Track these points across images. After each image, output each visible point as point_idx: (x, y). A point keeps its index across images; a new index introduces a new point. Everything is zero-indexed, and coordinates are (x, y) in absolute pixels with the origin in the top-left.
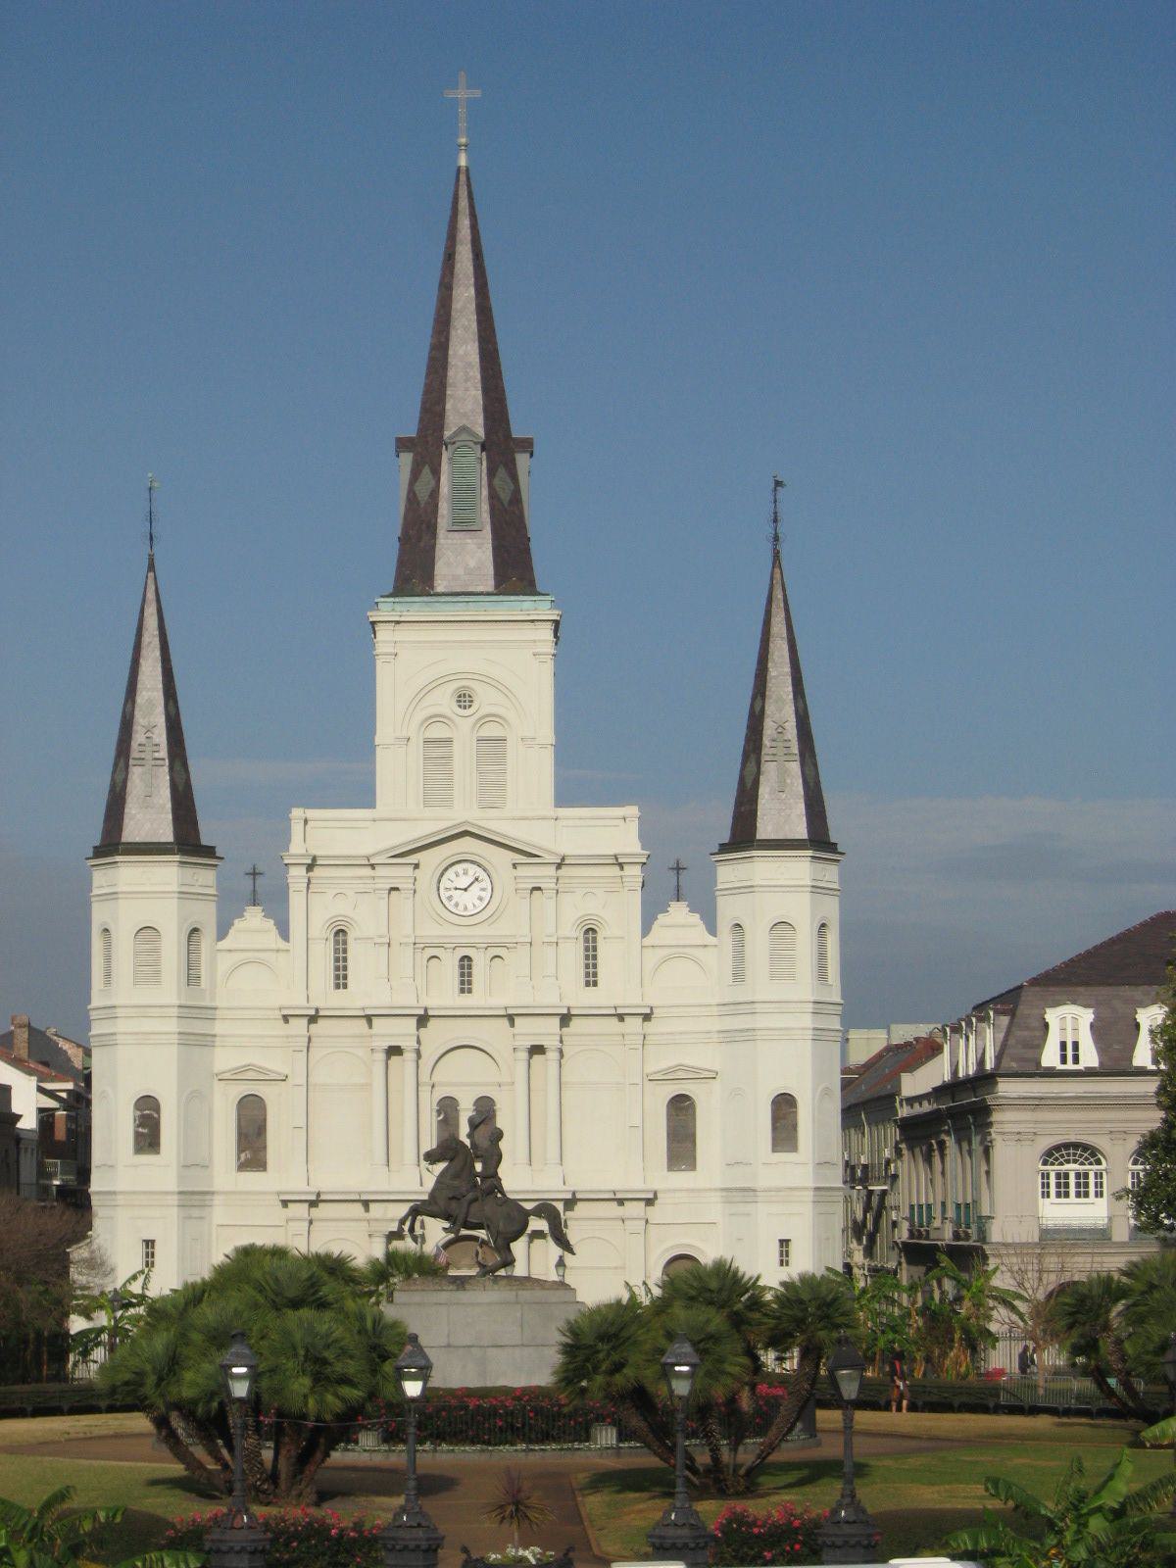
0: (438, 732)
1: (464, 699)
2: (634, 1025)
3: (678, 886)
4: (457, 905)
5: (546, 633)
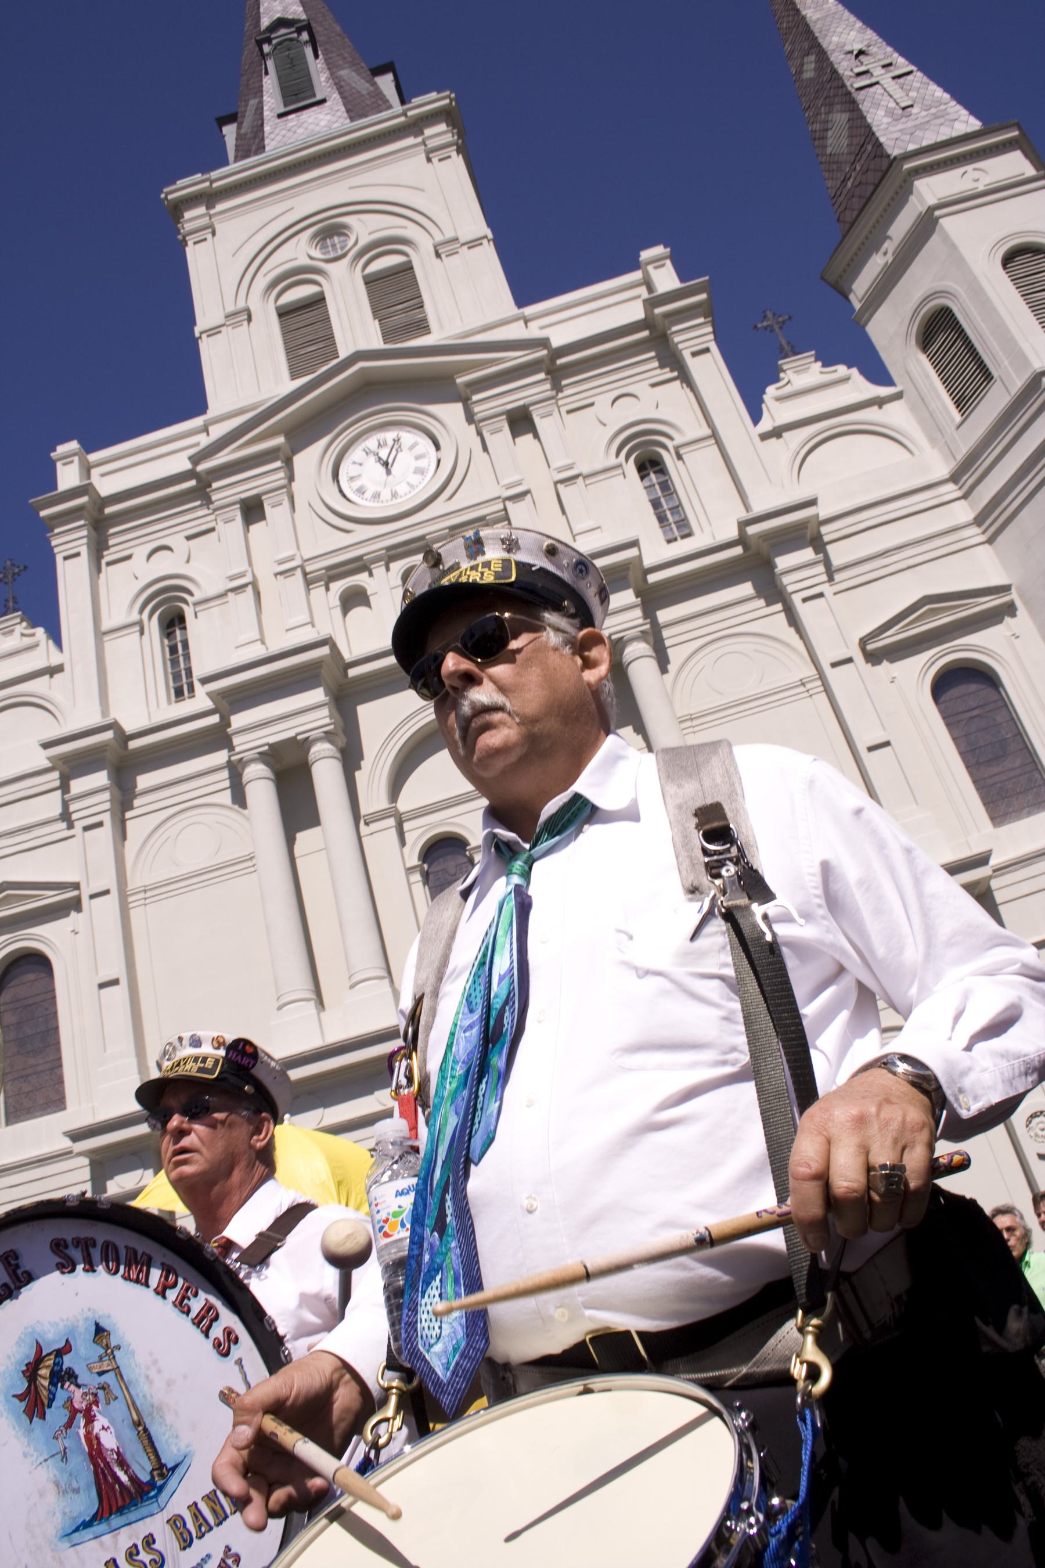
5: (439, 133)
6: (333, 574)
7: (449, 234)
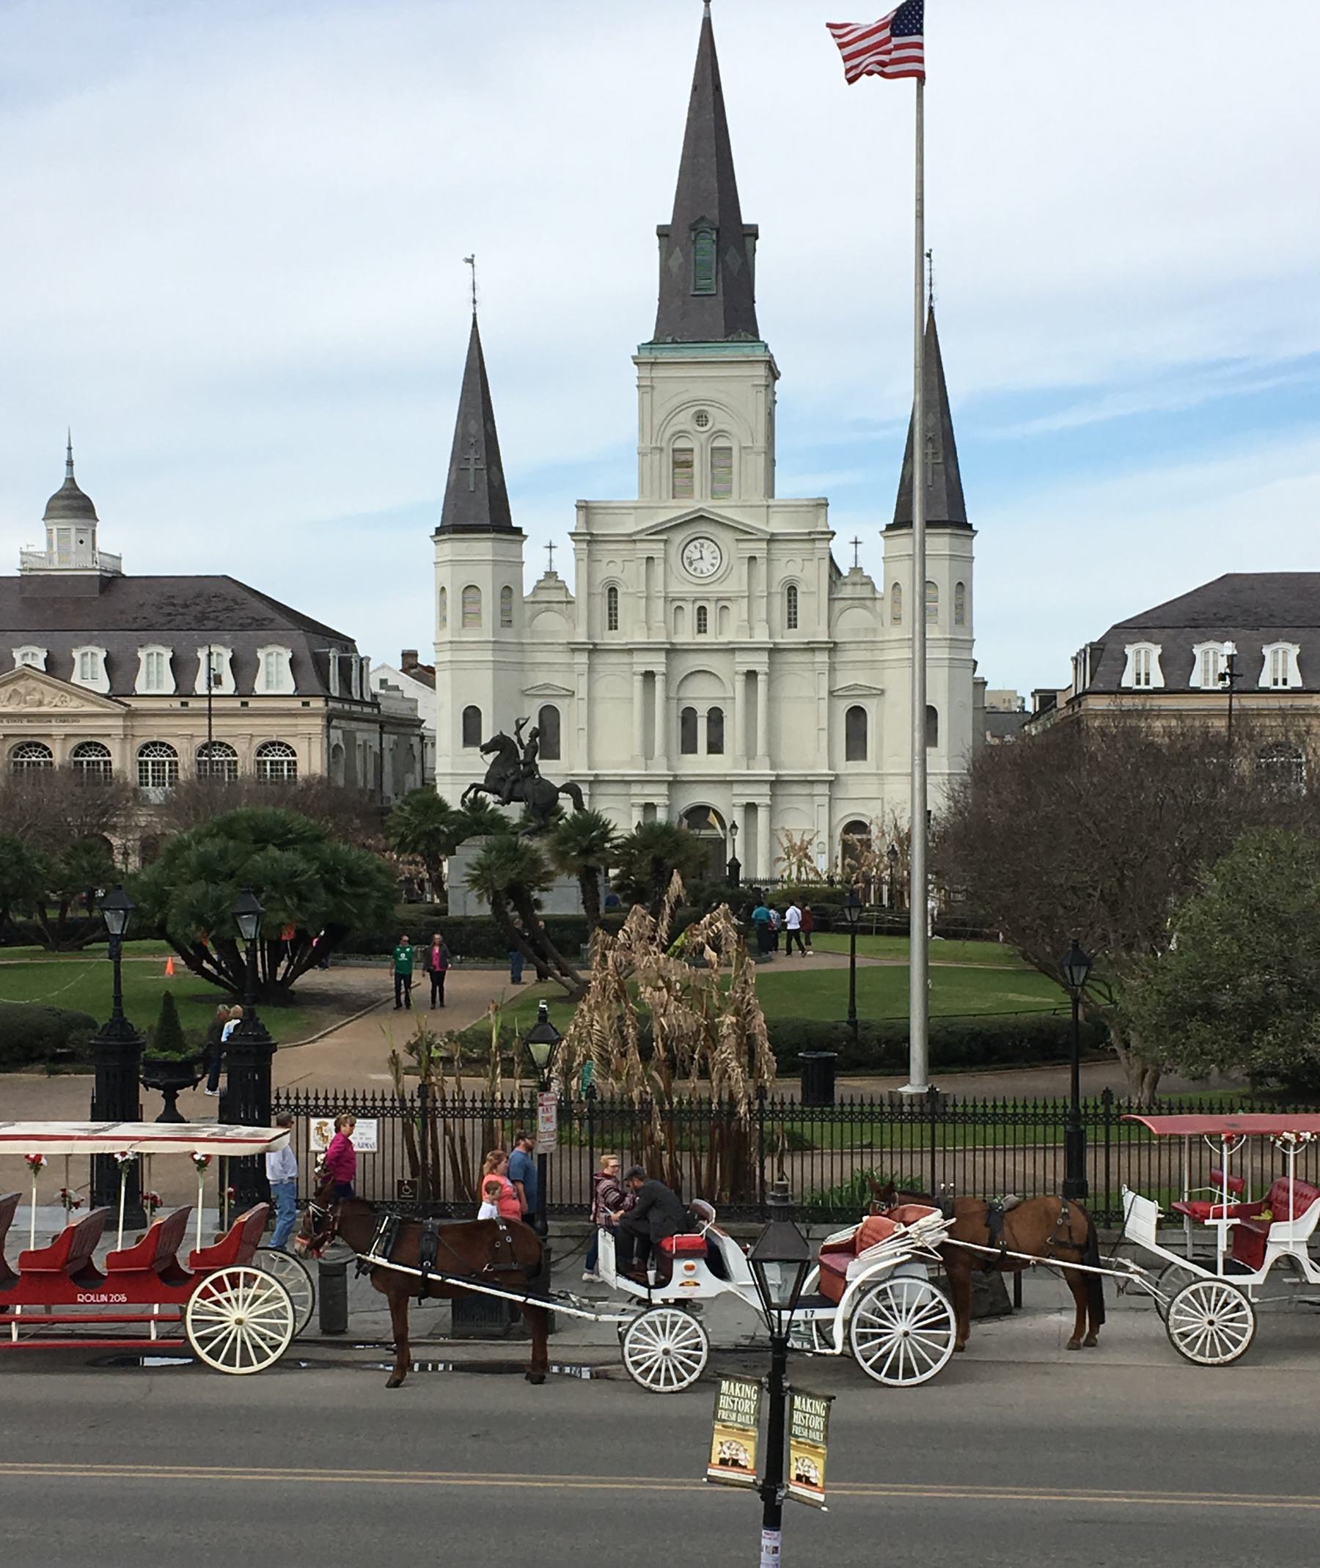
0: (681, 444)
1: (701, 418)
2: (823, 657)
3: (856, 556)
4: (695, 569)
6: (674, 599)
7: (750, 445)
